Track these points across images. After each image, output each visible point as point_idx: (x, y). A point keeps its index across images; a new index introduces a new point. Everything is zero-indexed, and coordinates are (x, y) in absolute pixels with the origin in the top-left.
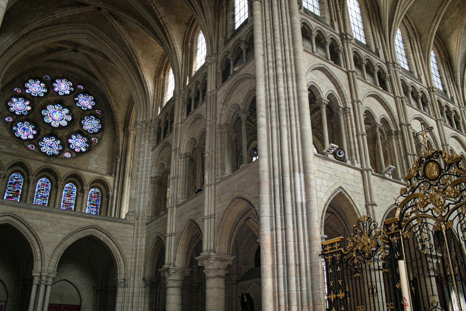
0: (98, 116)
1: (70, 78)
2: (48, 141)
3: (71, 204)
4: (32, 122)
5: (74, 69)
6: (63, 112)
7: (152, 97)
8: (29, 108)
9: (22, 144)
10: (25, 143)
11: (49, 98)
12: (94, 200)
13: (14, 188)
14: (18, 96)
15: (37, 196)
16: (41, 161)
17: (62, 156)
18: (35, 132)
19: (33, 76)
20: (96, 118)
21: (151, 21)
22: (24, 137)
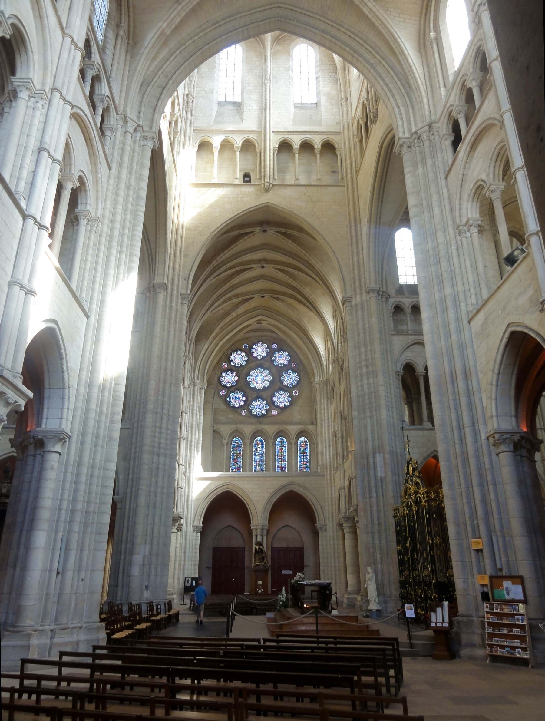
0: (295, 369)
1: (264, 341)
2: (256, 403)
3: (284, 456)
4: (241, 391)
5: (265, 333)
6: (264, 374)
7: (325, 357)
8: (236, 378)
9: (236, 412)
10: (239, 410)
11: (250, 365)
12: (303, 448)
13: (237, 451)
14: (226, 371)
15: (255, 454)
16: (252, 424)
17: (269, 414)
18: (244, 398)
19: (235, 349)
20: (294, 371)
21: (303, 300)
22: (237, 405)
